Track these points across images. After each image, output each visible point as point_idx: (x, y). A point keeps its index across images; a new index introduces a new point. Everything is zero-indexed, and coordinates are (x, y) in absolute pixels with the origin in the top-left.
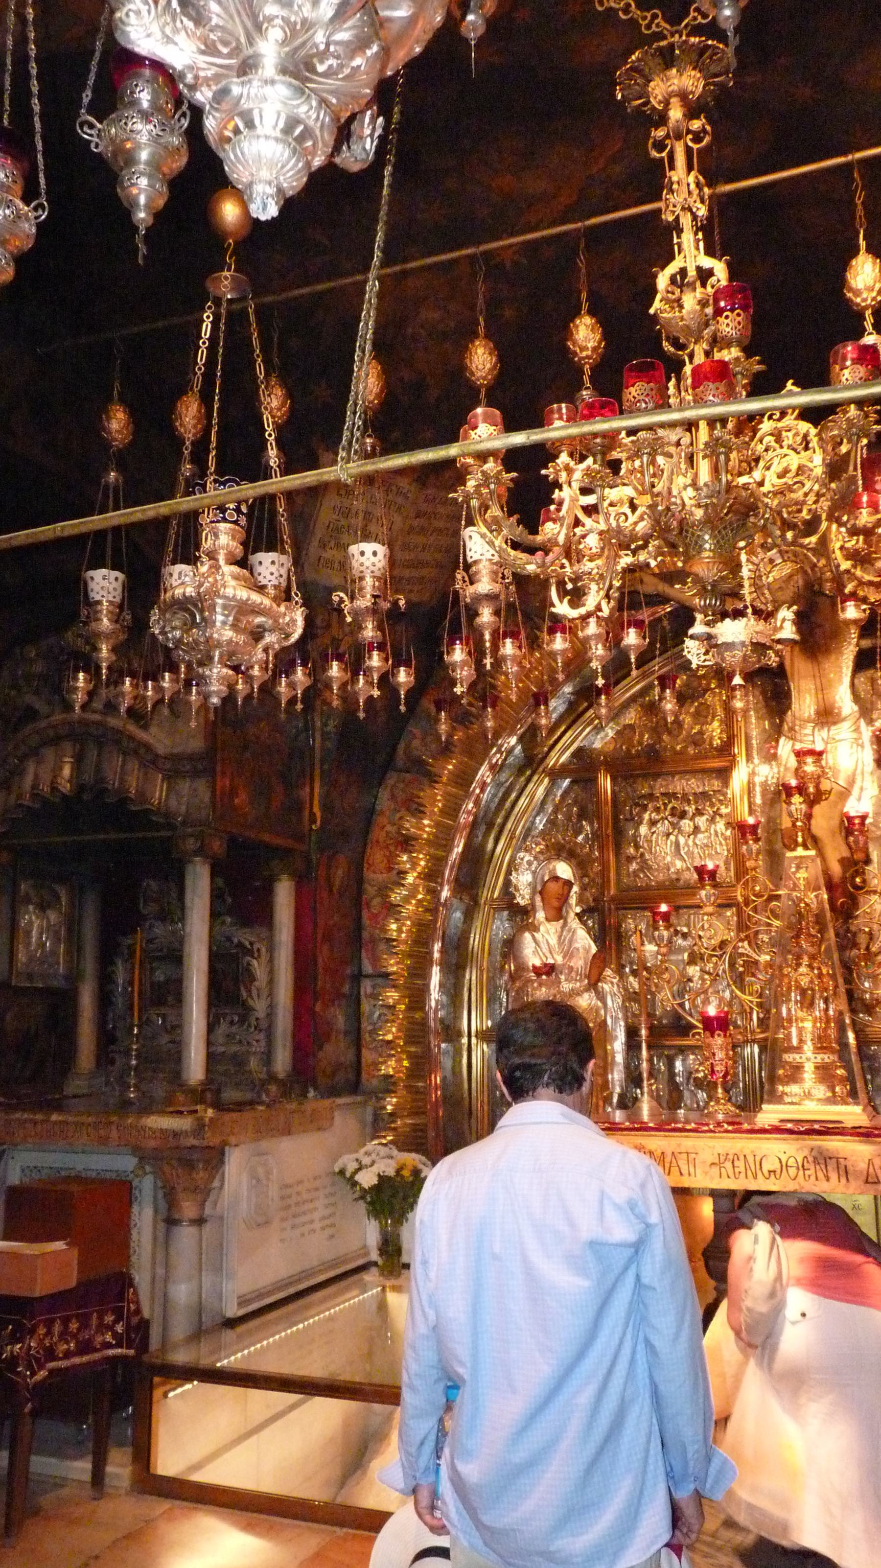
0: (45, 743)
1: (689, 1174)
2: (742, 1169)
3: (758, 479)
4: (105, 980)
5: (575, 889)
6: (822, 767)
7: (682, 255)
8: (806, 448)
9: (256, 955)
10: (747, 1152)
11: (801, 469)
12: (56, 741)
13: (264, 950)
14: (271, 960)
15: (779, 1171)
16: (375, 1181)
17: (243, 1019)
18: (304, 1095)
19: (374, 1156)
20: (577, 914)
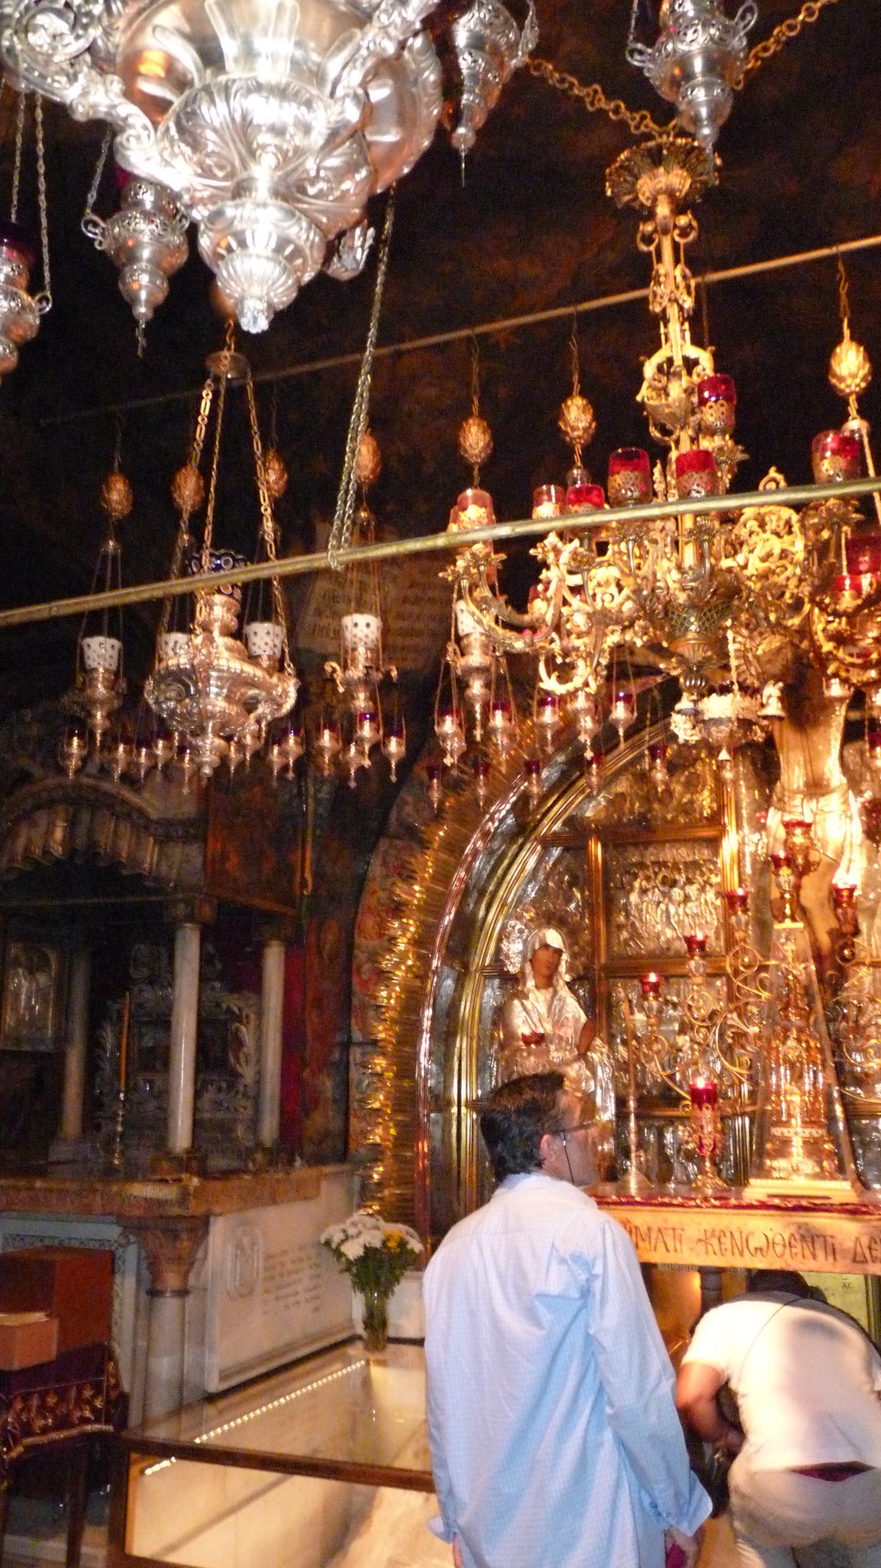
0: (37, 807)
1: (676, 1251)
2: (729, 1246)
3: (742, 563)
4: (93, 1044)
5: (565, 957)
6: (810, 838)
7: (669, 344)
8: (790, 532)
9: (245, 1021)
10: (733, 1228)
11: (784, 554)
12: (50, 804)
13: (252, 1017)
14: (259, 1027)
15: (765, 1249)
16: (361, 1252)
17: (232, 1086)
18: (291, 1162)
19: (360, 1227)
20: (567, 983)
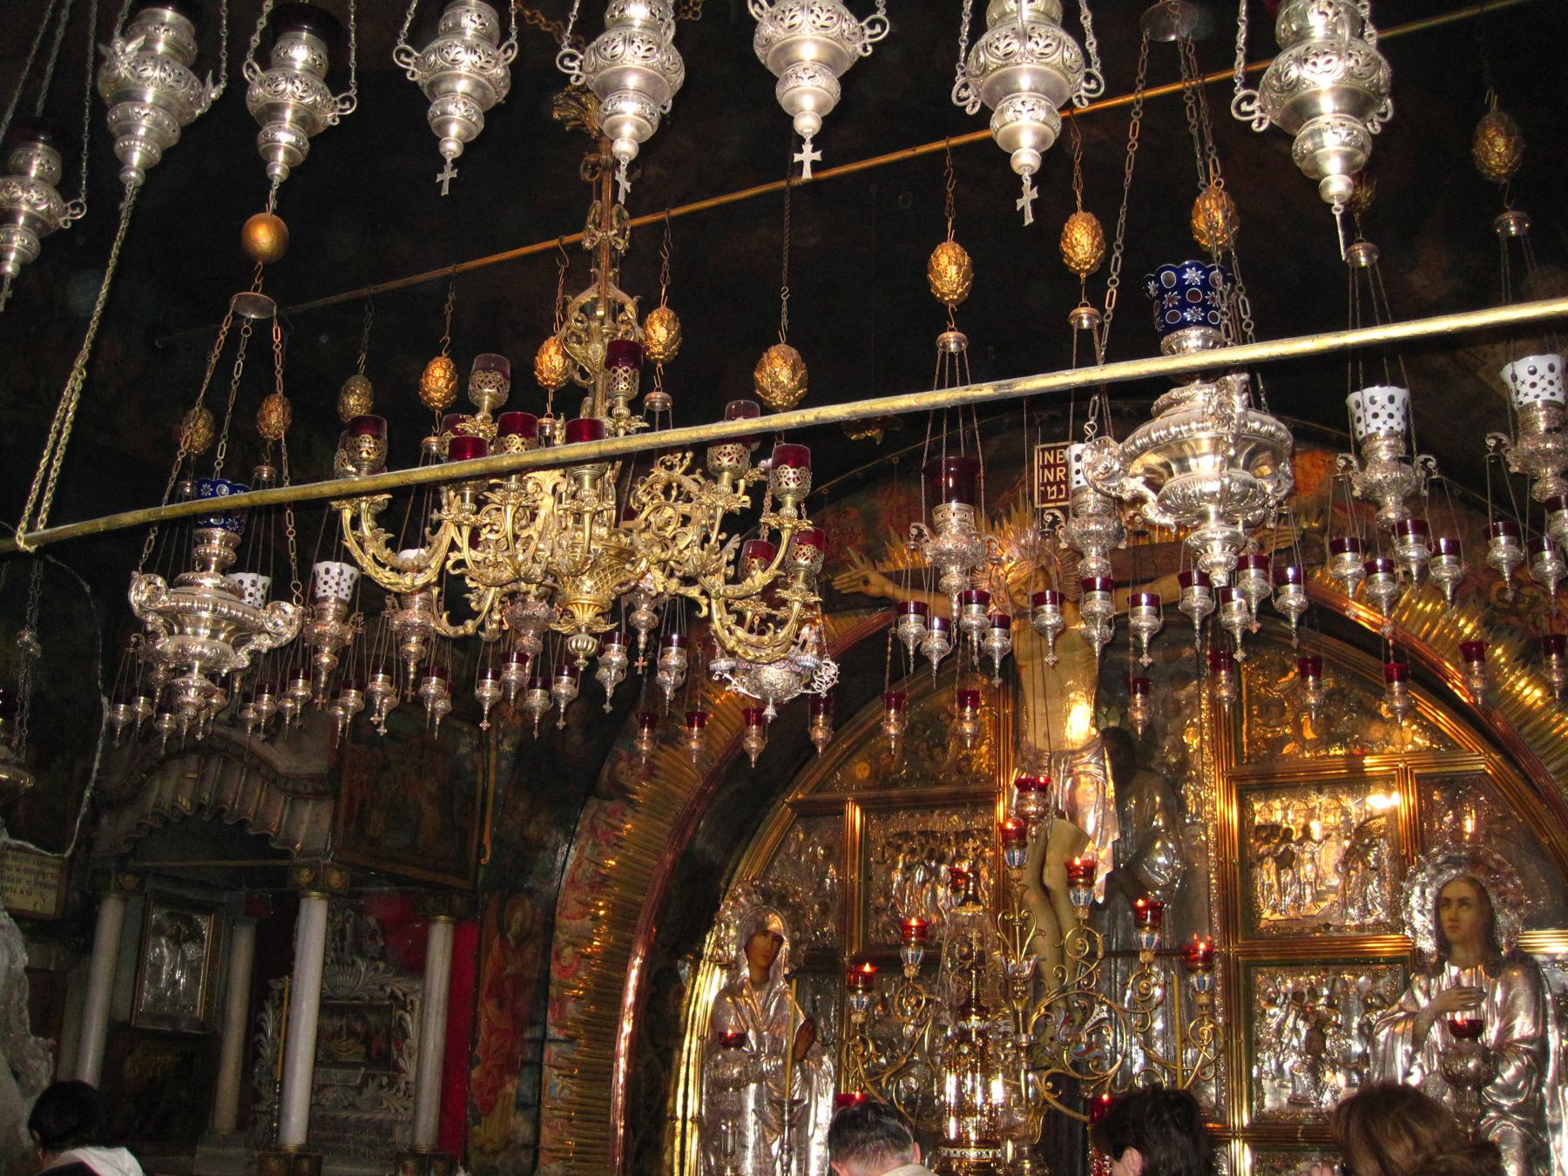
5: (786, 946)
9: (409, 1008)
17: (392, 1083)
20: (785, 976)
